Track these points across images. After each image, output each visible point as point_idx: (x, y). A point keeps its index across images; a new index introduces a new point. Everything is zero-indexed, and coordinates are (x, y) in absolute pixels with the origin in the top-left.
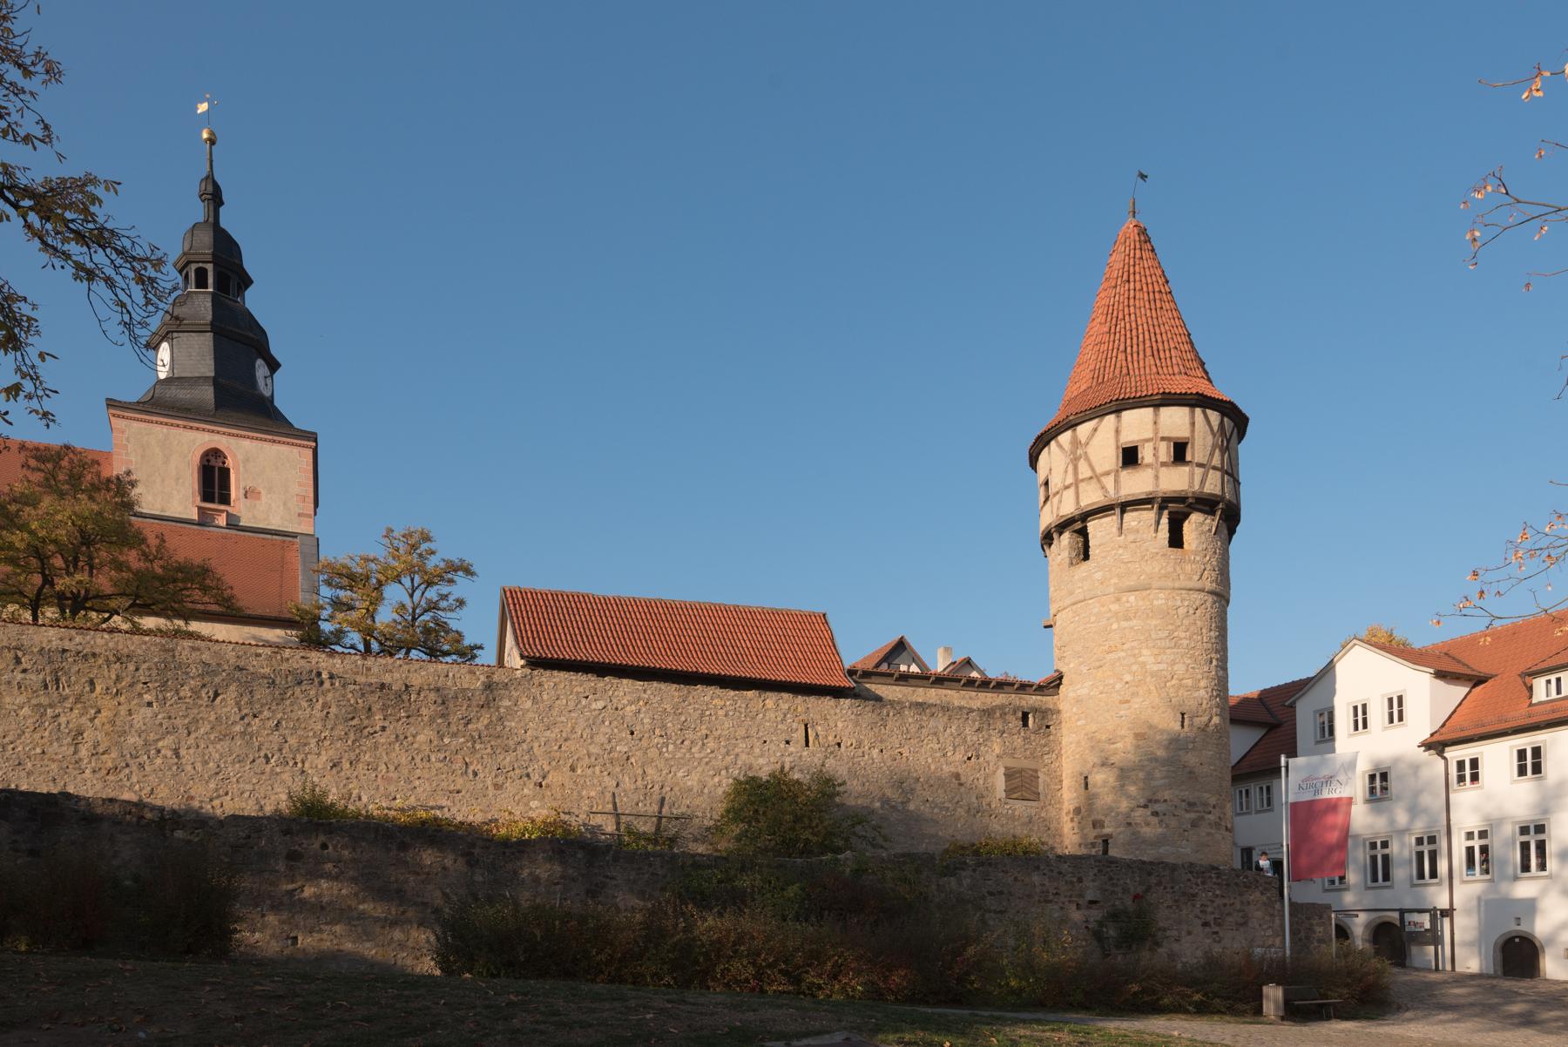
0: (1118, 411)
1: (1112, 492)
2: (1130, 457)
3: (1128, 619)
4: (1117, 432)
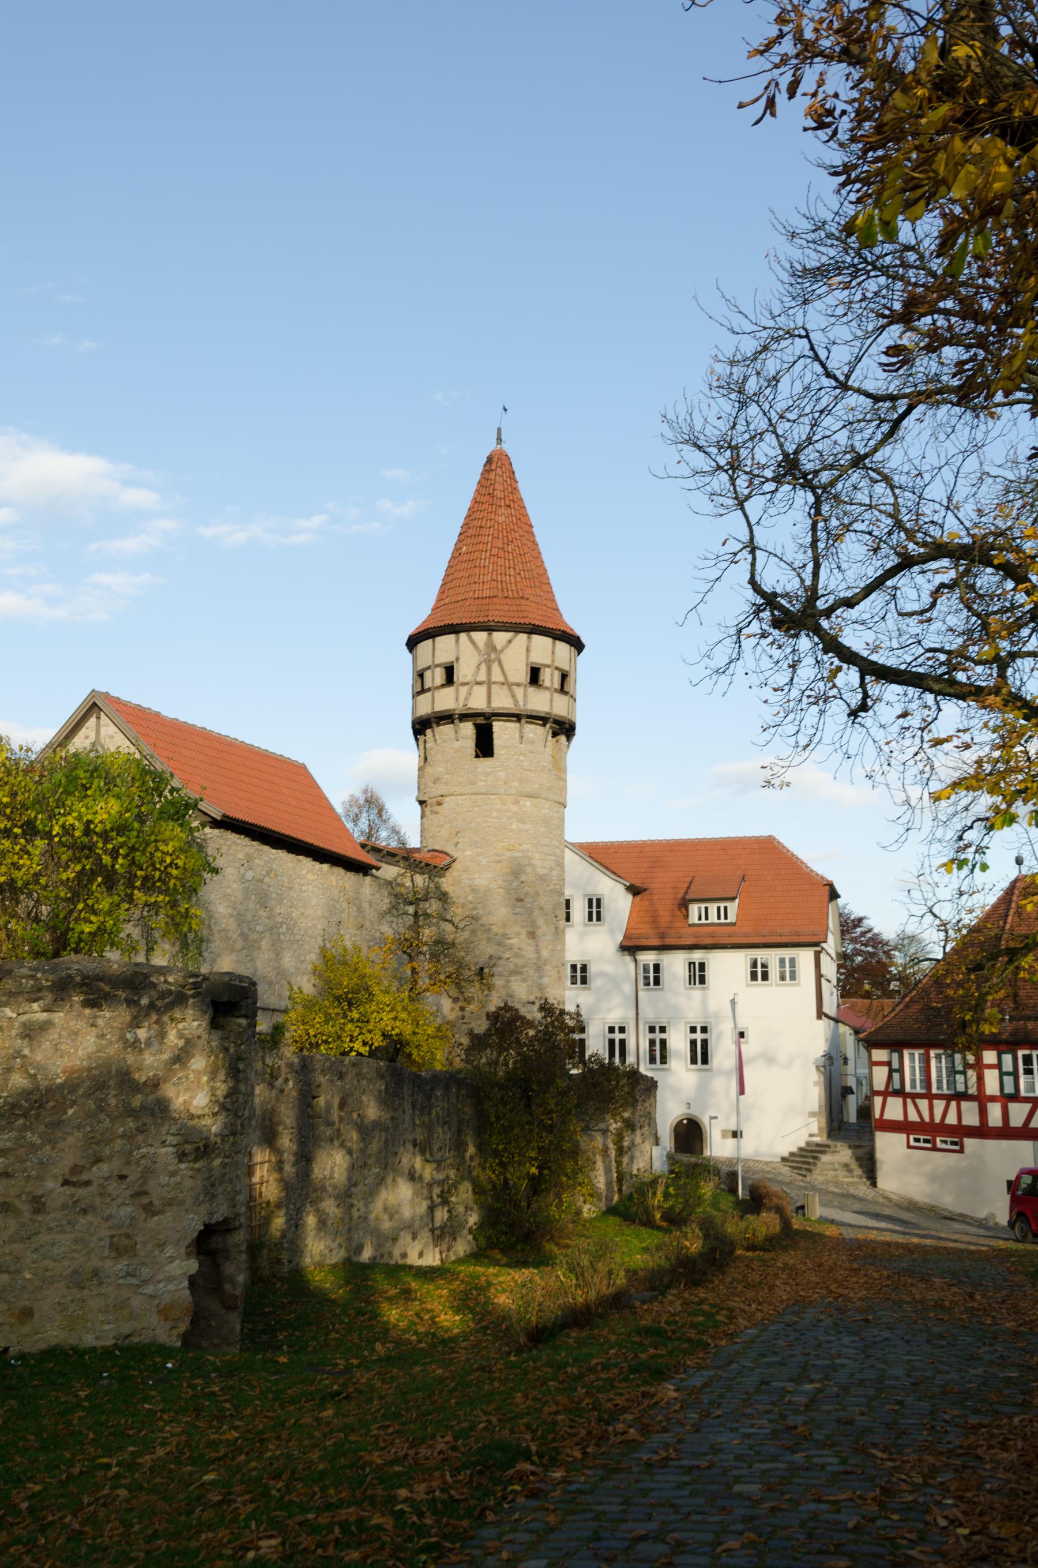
0: (530, 633)
1: (521, 703)
2: (535, 675)
3: (524, 823)
4: (528, 650)
